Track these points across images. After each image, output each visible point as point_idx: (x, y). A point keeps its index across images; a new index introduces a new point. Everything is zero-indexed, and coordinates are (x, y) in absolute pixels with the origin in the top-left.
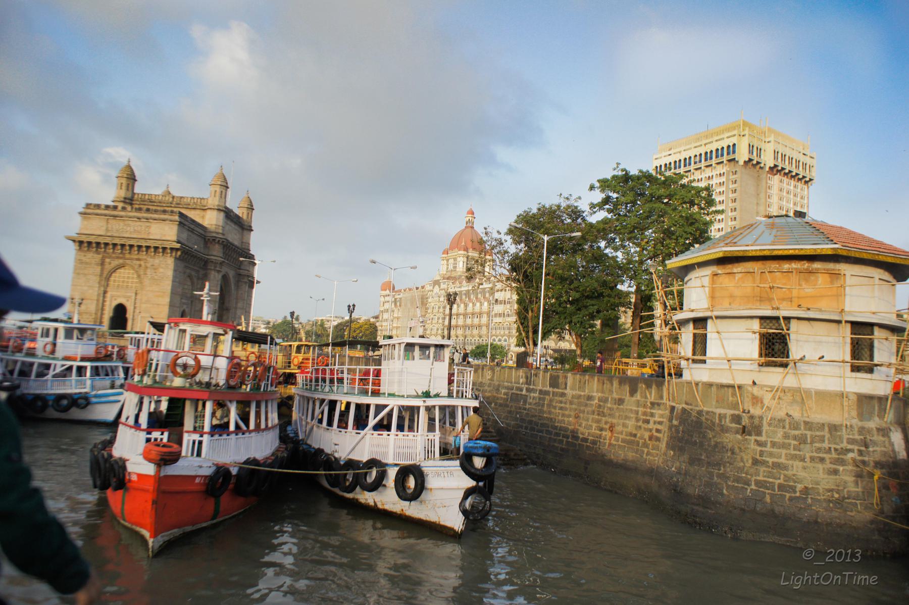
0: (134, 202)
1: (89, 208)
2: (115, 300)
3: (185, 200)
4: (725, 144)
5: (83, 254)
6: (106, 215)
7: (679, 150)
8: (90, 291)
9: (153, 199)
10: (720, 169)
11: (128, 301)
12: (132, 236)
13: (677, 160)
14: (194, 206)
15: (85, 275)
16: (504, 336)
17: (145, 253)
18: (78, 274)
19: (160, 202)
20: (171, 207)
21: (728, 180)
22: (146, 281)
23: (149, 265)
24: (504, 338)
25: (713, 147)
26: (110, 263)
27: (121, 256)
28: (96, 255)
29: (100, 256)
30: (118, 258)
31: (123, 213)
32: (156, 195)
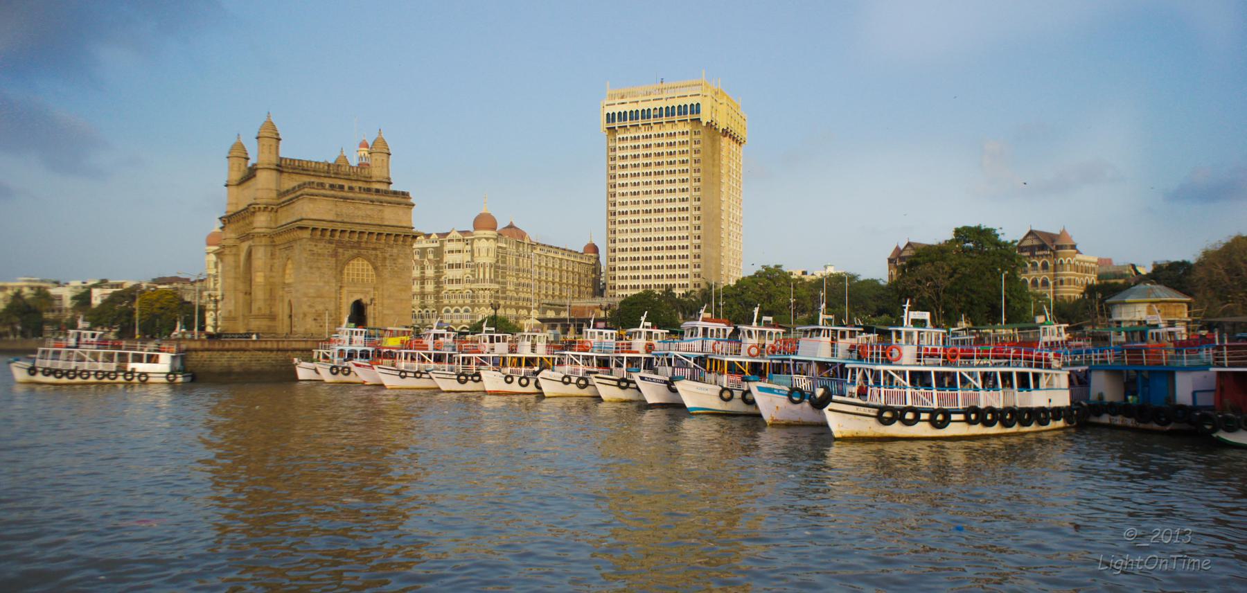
0: (285, 170)
1: (314, 188)
2: (352, 296)
3: (343, 169)
4: (688, 102)
5: (314, 244)
6: (336, 198)
7: (636, 99)
8: (327, 288)
9: (305, 166)
10: (681, 128)
11: (366, 297)
12: (365, 222)
13: (634, 110)
14: (355, 177)
15: (319, 268)
16: (464, 306)
17: (383, 241)
18: (311, 268)
19: (314, 171)
20: (330, 177)
21: (691, 139)
22: (386, 273)
23: (387, 255)
24: (464, 308)
25: (676, 103)
26: (343, 254)
27: (356, 245)
28: (327, 245)
29: (334, 246)
30: (352, 247)
31: (351, 195)
32: (307, 162)
